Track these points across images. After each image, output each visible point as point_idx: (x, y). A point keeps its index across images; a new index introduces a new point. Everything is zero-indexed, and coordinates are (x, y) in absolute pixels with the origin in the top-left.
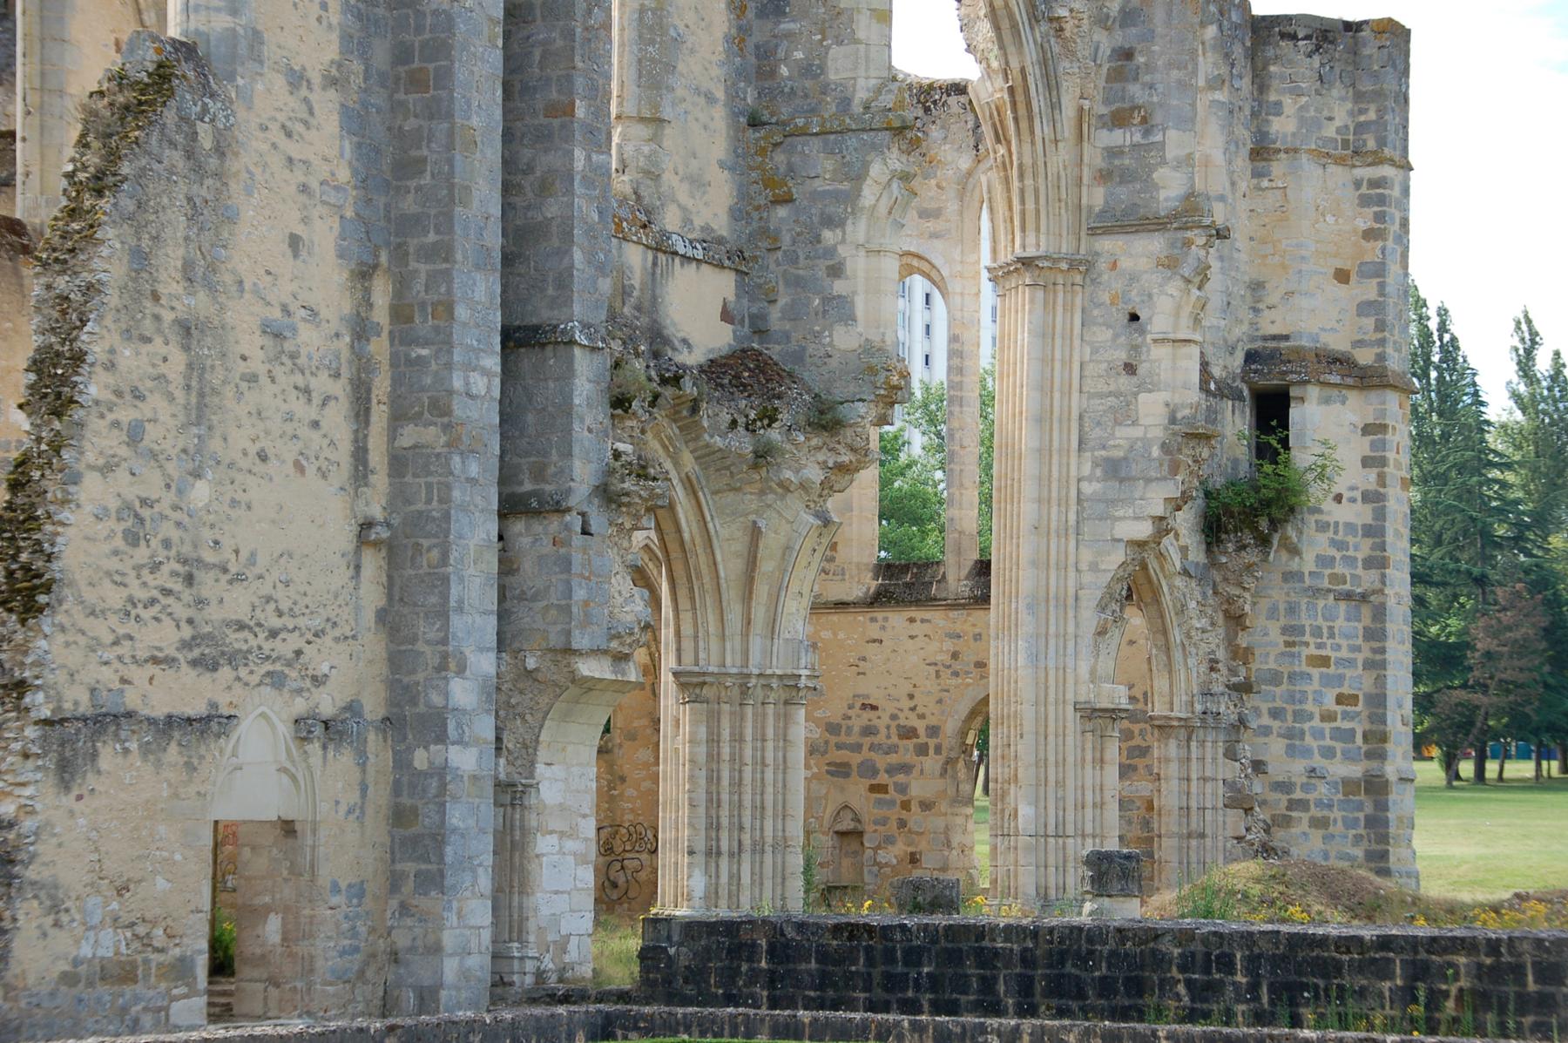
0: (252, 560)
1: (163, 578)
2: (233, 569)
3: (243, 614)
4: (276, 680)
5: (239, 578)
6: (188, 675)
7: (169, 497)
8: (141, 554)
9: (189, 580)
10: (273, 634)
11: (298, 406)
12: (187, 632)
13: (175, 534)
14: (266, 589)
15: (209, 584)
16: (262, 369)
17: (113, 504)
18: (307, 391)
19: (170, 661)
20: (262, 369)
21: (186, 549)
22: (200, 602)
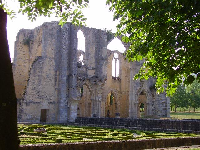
4: (47, 100)
11: (49, 81)
15: (40, 93)
18: (50, 80)
22: (40, 94)
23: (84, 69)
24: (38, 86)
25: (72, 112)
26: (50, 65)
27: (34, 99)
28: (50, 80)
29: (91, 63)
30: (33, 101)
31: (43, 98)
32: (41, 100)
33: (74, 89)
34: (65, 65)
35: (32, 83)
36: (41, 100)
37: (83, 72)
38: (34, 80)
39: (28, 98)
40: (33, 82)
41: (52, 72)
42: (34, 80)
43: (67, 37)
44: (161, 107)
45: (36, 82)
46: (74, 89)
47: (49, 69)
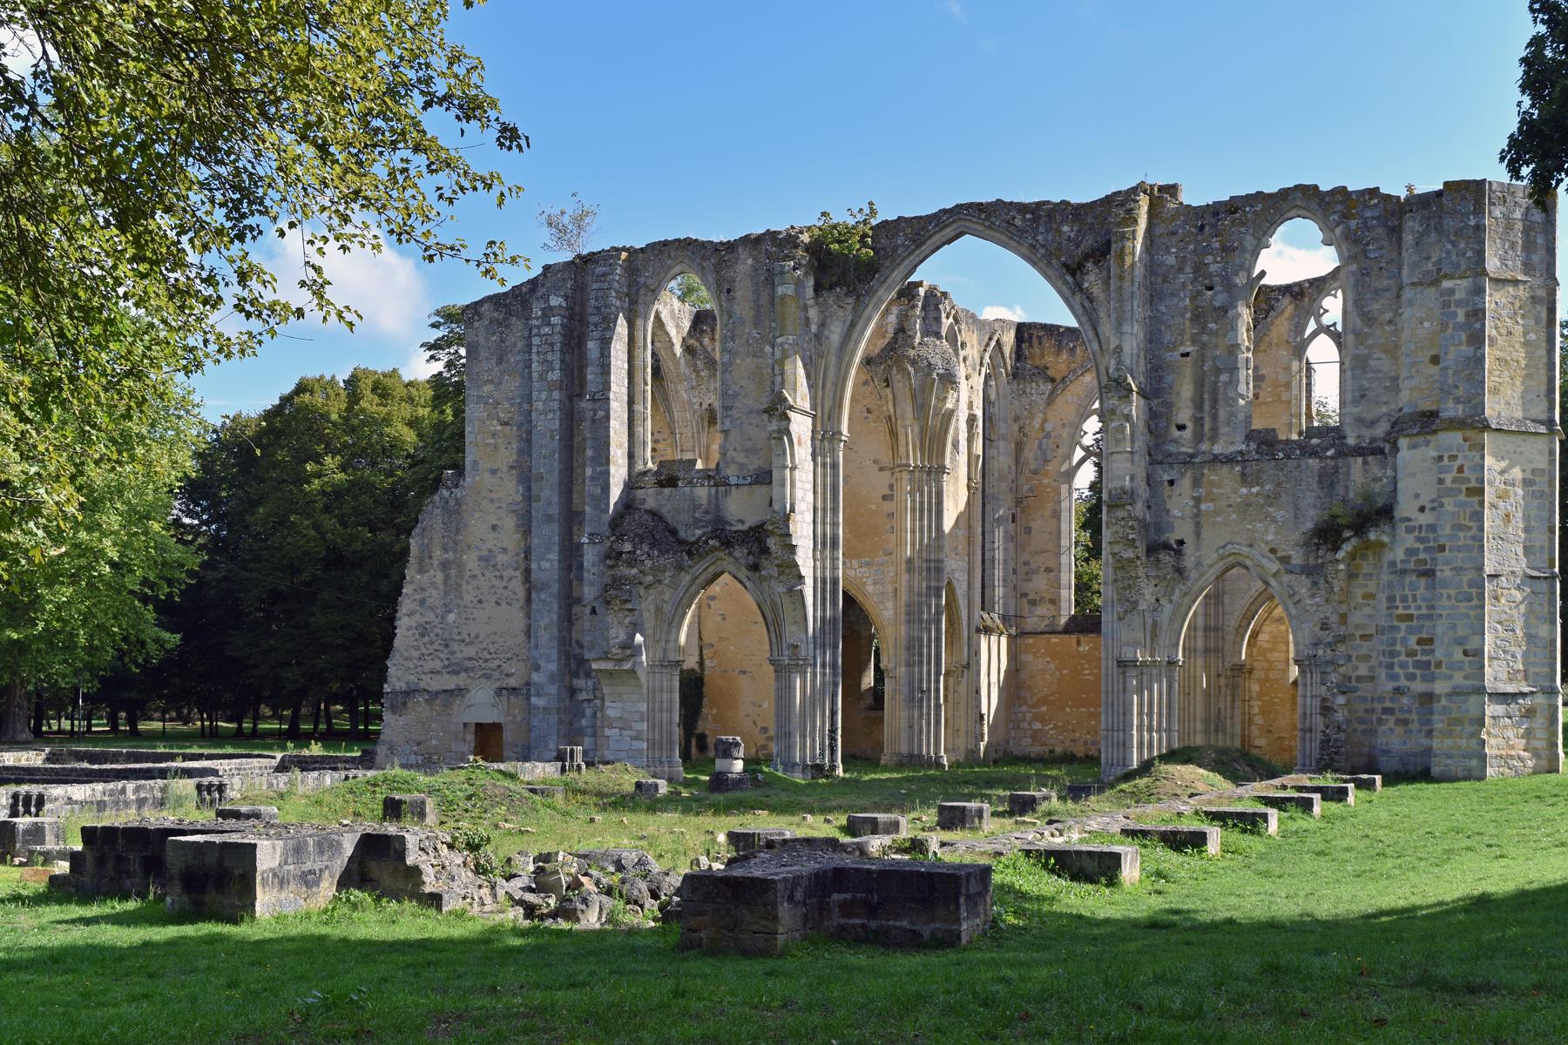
0: (477, 636)
1: (435, 646)
3: (473, 654)
4: (487, 677)
5: (471, 643)
6: (447, 677)
8: (426, 639)
9: (447, 646)
11: (497, 583)
15: (455, 647)
16: (478, 573)
18: (501, 577)
19: (438, 672)
20: (478, 573)
22: (453, 653)
23: (702, 492)
24: (443, 618)
25: (607, 732)
27: (426, 678)
28: (501, 577)
29: (749, 444)
31: (466, 670)
32: (460, 680)
33: (593, 611)
34: (549, 495)
36: (460, 680)
37: (695, 508)
38: (423, 589)
39: (399, 673)
41: (509, 537)
42: (423, 589)
43: (552, 345)
44: (1403, 682)
45: (435, 598)
46: (593, 611)
47: (494, 527)
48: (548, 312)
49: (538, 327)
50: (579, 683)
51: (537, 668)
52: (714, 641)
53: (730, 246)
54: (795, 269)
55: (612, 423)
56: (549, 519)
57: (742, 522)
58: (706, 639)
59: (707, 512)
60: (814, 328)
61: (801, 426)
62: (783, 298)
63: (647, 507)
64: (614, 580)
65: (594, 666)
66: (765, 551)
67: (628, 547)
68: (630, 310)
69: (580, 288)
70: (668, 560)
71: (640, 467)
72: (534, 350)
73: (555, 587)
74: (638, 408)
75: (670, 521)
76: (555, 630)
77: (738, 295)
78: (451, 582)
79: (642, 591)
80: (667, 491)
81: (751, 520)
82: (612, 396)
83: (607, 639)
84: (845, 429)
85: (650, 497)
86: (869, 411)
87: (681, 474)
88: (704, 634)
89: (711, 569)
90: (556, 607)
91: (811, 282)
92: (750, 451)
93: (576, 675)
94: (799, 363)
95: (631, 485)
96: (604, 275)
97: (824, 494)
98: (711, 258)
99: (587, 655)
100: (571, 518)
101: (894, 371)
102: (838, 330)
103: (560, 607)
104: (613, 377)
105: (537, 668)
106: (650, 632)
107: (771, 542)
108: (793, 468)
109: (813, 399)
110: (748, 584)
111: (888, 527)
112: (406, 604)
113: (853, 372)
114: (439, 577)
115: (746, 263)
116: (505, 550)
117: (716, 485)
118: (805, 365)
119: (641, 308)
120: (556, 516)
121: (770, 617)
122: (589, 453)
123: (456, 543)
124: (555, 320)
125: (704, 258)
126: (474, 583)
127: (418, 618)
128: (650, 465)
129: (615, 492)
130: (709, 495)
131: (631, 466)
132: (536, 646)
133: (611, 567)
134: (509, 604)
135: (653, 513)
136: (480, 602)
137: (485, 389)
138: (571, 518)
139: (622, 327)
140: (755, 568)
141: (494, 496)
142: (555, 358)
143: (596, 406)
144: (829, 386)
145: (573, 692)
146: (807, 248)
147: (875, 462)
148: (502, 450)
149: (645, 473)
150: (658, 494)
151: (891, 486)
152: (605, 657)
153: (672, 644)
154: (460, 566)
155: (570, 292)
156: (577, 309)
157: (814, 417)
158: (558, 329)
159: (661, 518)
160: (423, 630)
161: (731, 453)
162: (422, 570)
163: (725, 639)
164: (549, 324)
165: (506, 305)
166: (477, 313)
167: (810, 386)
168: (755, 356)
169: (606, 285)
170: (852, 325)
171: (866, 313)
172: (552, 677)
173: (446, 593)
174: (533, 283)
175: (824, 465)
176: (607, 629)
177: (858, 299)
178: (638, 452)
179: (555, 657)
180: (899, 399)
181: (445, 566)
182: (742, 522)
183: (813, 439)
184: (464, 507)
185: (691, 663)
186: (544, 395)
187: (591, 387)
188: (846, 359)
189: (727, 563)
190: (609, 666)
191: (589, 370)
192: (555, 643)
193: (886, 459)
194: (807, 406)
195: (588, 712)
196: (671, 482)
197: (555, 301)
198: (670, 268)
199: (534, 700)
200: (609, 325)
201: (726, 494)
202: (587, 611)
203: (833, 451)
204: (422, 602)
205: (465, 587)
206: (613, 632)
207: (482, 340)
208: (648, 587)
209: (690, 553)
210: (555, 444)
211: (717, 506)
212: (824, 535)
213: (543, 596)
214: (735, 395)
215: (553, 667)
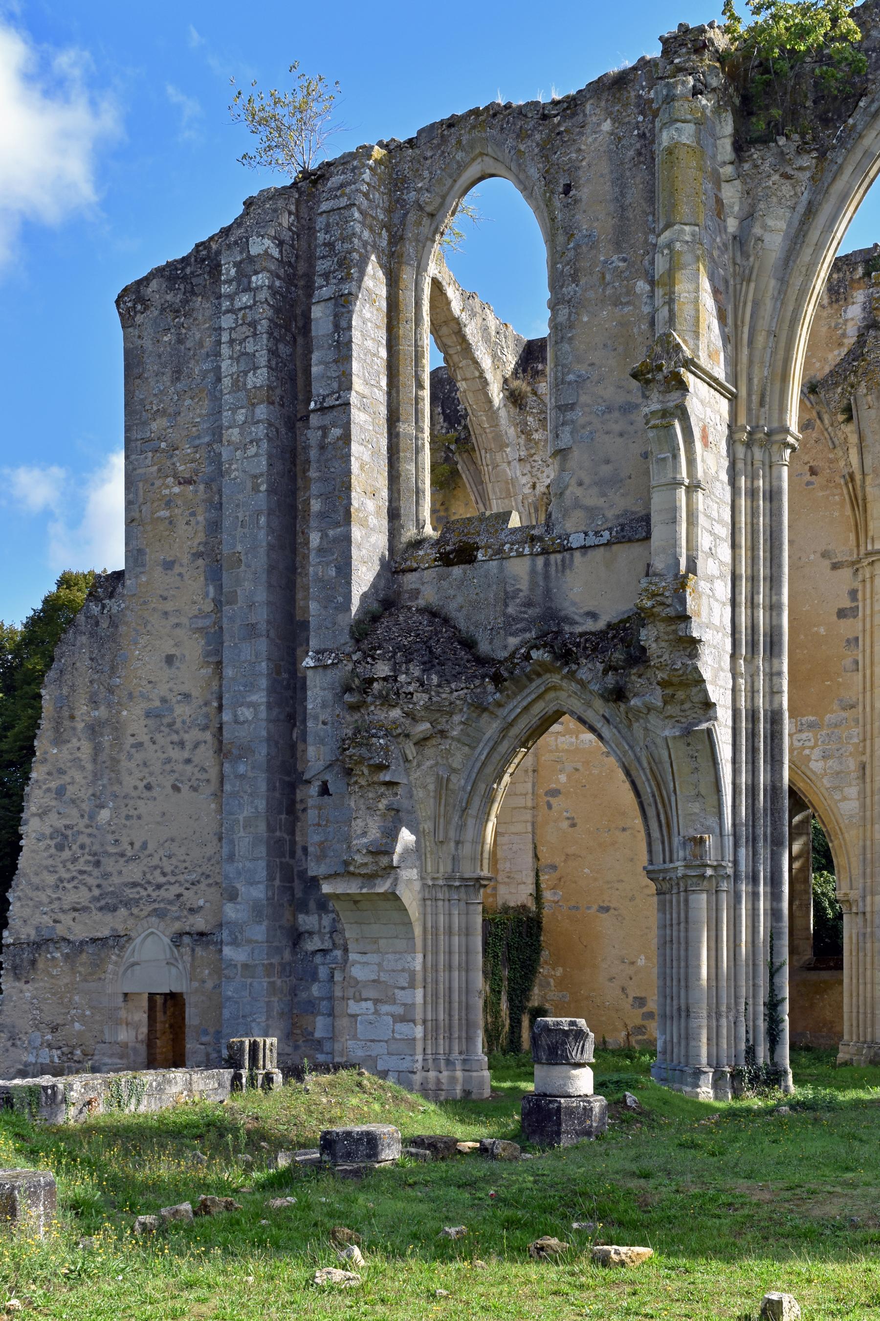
0: (144, 846)
1: (81, 865)
2: (129, 853)
3: (137, 877)
4: (160, 914)
5: (134, 858)
6: (97, 916)
7: (82, 823)
8: (67, 854)
9: (97, 864)
10: (159, 887)
11: (175, 754)
12: (96, 892)
13: (87, 841)
14: (155, 861)
15: (109, 864)
16: (145, 739)
17: (48, 831)
18: (182, 744)
20: (145, 739)
21: (95, 848)
22: (106, 875)
23: (520, 569)
24: (92, 817)
26: (173, 620)
28: (182, 744)
30: (60, 930)
31: (127, 904)
33: (325, 791)
34: (252, 589)
35: (49, 801)
37: (507, 598)
38: (62, 772)
40: (53, 785)
42: (62, 772)
45: (79, 783)
46: (325, 791)
47: (170, 660)
48: (247, 266)
49: (231, 297)
50: (308, 921)
51: (233, 896)
52: (558, 860)
53: (571, 105)
54: (696, 92)
55: (355, 448)
56: (251, 631)
57: (593, 615)
58: (546, 856)
59: (529, 604)
60: (732, 224)
61: (707, 408)
62: (670, 151)
63: (421, 602)
64: (357, 731)
65: (326, 888)
66: (638, 657)
67: (383, 669)
68: (392, 255)
69: (305, 229)
70: (456, 693)
71: (409, 533)
72: (225, 338)
73: (262, 752)
74: (406, 428)
75: (462, 624)
76: (262, 827)
77: (584, 193)
78: (103, 757)
79: (411, 750)
80: (457, 571)
81: (611, 609)
82: (354, 399)
83: (348, 840)
84: (793, 421)
85: (427, 587)
86: (813, 472)
87: (482, 540)
88: (543, 850)
89: (538, 709)
90: (263, 787)
91: (727, 127)
92: (603, 484)
93: (301, 906)
94: (705, 284)
95: (393, 567)
96: (342, 186)
97: (753, 548)
98: (529, 138)
99: (314, 869)
100: (290, 632)
101: (862, 390)
102: (782, 225)
103: (271, 788)
104: (355, 366)
105: (233, 896)
106: (428, 826)
107: (648, 636)
108: (694, 487)
109: (733, 363)
110: (606, 732)
111: (848, 662)
112: (36, 798)
113: (810, 310)
114: (86, 748)
115: (600, 128)
116: (187, 696)
117: (545, 552)
118: (716, 292)
119: (410, 248)
120: (263, 627)
121: (647, 789)
122: (316, 506)
123: (111, 691)
124: (257, 280)
125: (522, 135)
126: (139, 757)
127: (54, 820)
128: (428, 530)
129: (364, 576)
130: (533, 572)
131: (393, 533)
132: (231, 858)
133: (354, 708)
134: (195, 789)
135: (432, 613)
136: (148, 787)
137: (154, 426)
138: (290, 632)
139: (374, 280)
140: (618, 695)
141: (169, 606)
142: (259, 347)
143: (327, 419)
144: (761, 339)
145: (296, 937)
146: (722, 58)
147: (825, 555)
148: (181, 527)
149: (417, 544)
150: (441, 578)
151: (853, 594)
152: (346, 872)
153: (467, 849)
154: (117, 727)
155: (286, 235)
156: (302, 268)
157: (733, 399)
158: (263, 295)
159: (446, 621)
160: (61, 840)
161: (573, 491)
162: (59, 740)
163: (576, 856)
164: (248, 289)
165: (185, 278)
166: (141, 299)
167: (726, 339)
168: (617, 302)
169: (344, 202)
170: (811, 211)
171: (839, 185)
172: (257, 910)
173: (96, 776)
174: (226, 232)
175: (752, 493)
176: (349, 822)
177: (822, 156)
178: (407, 506)
179: (262, 874)
180: (869, 438)
181: (94, 730)
182: (593, 615)
183: (731, 441)
184: (123, 629)
185: (517, 893)
186: (240, 416)
187: (318, 389)
188: (796, 281)
189: (567, 695)
190: (352, 888)
191: (315, 356)
192: (262, 851)
193: (844, 550)
194: (720, 372)
195: (323, 972)
196: (464, 555)
197: (257, 246)
198: (462, 167)
199: (227, 951)
200: (348, 270)
201: (564, 566)
202: (314, 789)
203: (771, 466)
204: (60, 792)
205: (125, 764)
206: (358, 826)
207: (147, 343)
208: (422, 742)
209: (497, 679)
210: (261, 500)
211: (548, 593)
212: (753, 628)
213: (242, 769)
214: (581, 382)
215: (259, 892)
